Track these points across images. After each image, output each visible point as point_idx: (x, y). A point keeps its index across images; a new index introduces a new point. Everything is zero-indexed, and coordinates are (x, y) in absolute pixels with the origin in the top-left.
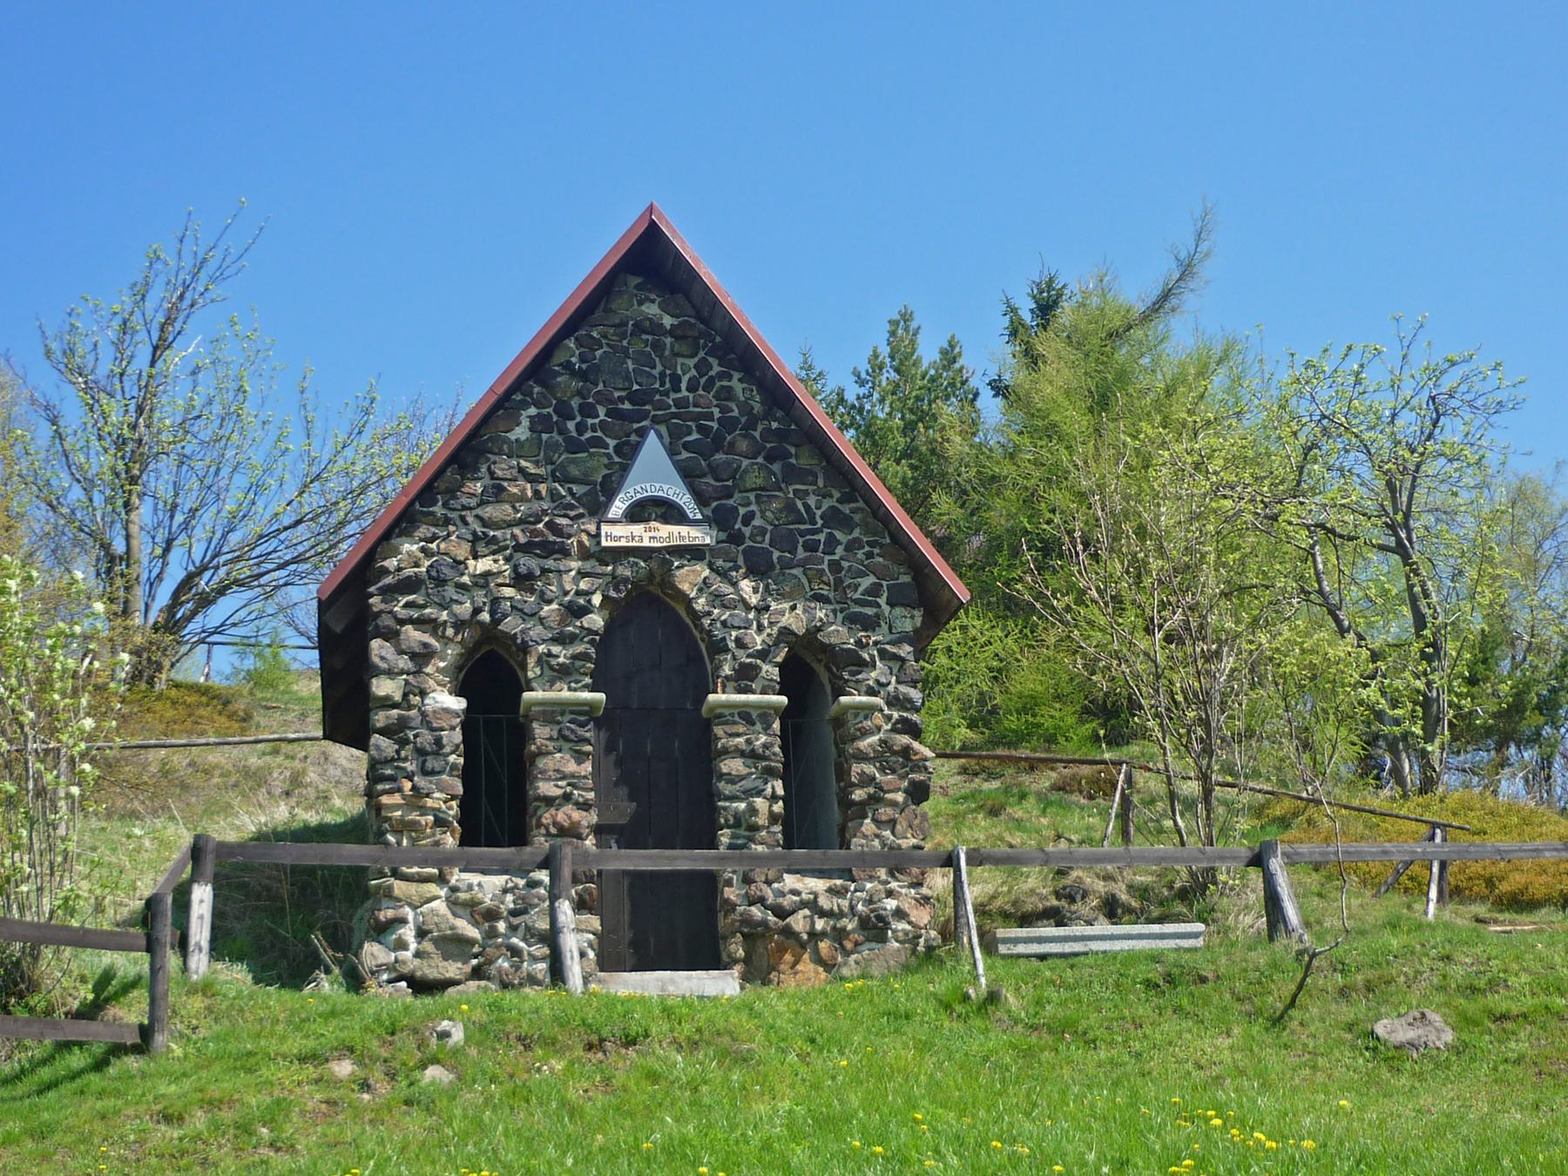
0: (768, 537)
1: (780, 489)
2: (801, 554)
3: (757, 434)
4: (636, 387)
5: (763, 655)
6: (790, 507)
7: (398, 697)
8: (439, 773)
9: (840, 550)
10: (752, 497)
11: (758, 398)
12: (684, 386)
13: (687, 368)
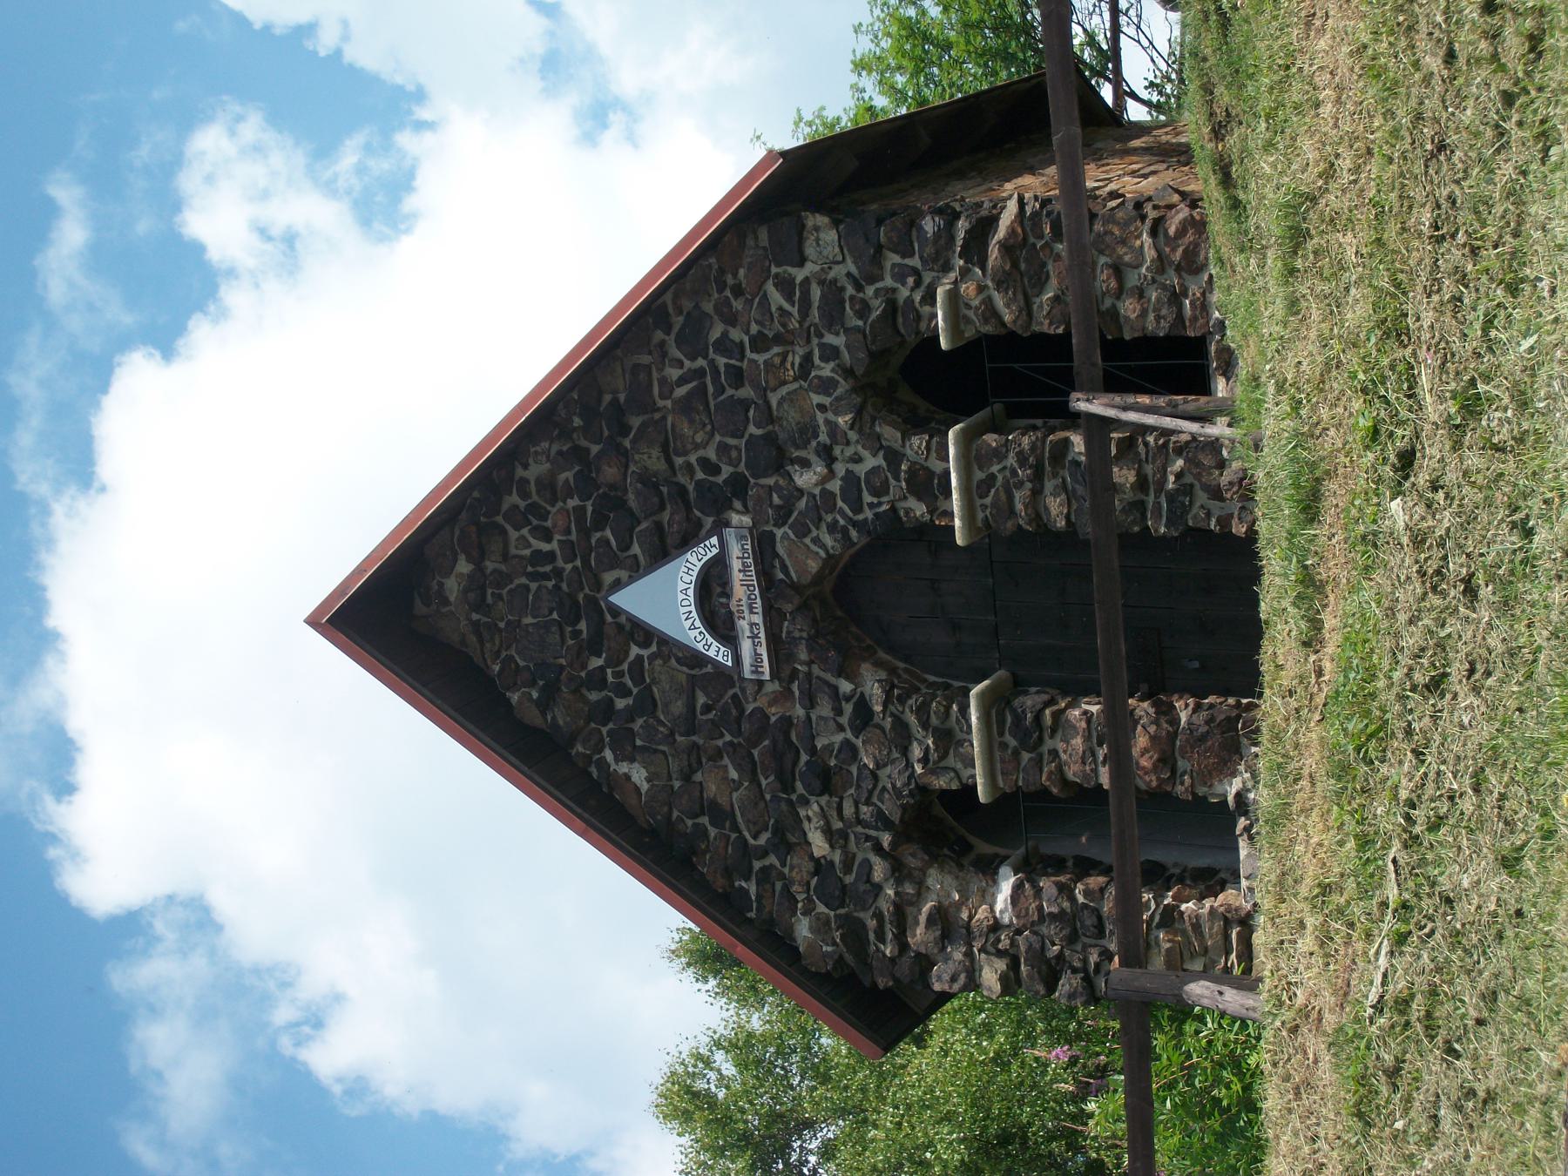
0: (732, 441)
1: (664, 418)
2: (746, 392)
3: (595, 449)
4: (555, 616)
5: (894, 458)
6: (685, 406)
7: (1001, 965)
8: (1100, 918)
9: (736, 334)
10: (679, 461)
11: (545, 445)
12: (545, 547)
13: (523, 542)
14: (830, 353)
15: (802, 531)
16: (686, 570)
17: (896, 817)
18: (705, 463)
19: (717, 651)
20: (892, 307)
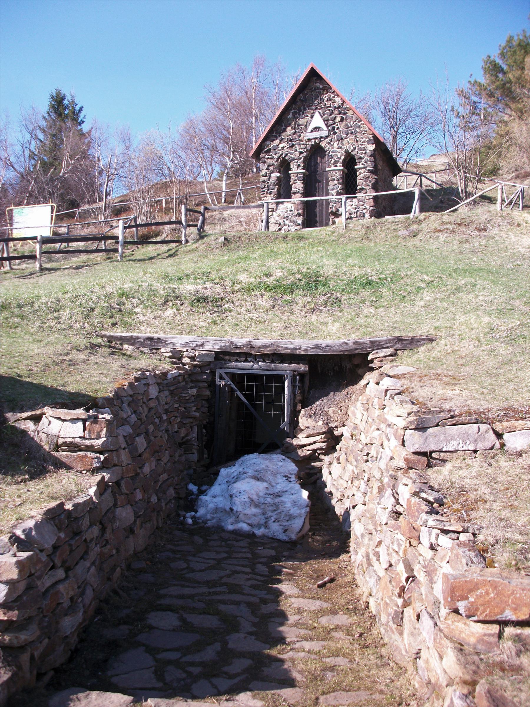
6: (346, 125)
14: (355, 148)
15: (329, 143)
16: (322, 125)
17: (286, 158)
18: (338, 128)
19: (309, 129)
20: (361, 158)
